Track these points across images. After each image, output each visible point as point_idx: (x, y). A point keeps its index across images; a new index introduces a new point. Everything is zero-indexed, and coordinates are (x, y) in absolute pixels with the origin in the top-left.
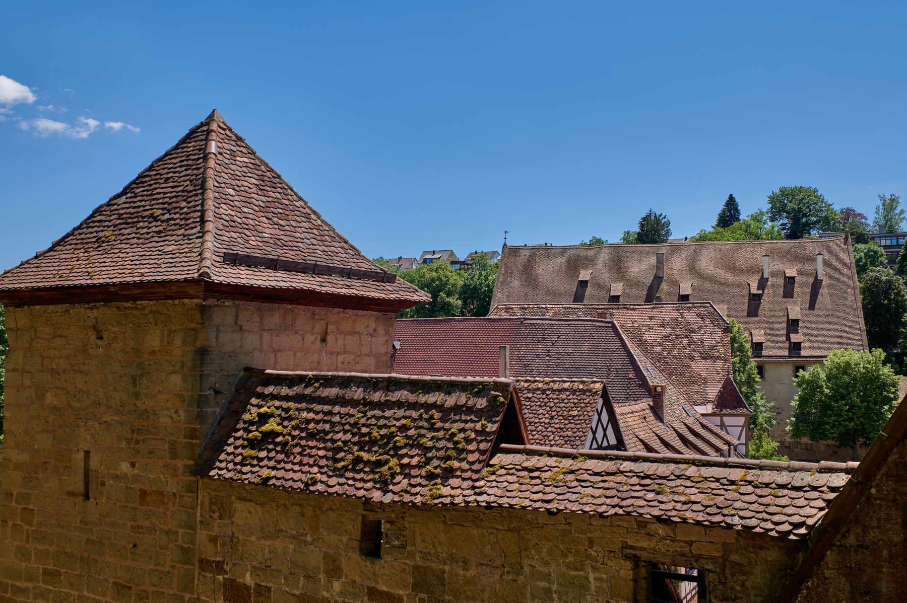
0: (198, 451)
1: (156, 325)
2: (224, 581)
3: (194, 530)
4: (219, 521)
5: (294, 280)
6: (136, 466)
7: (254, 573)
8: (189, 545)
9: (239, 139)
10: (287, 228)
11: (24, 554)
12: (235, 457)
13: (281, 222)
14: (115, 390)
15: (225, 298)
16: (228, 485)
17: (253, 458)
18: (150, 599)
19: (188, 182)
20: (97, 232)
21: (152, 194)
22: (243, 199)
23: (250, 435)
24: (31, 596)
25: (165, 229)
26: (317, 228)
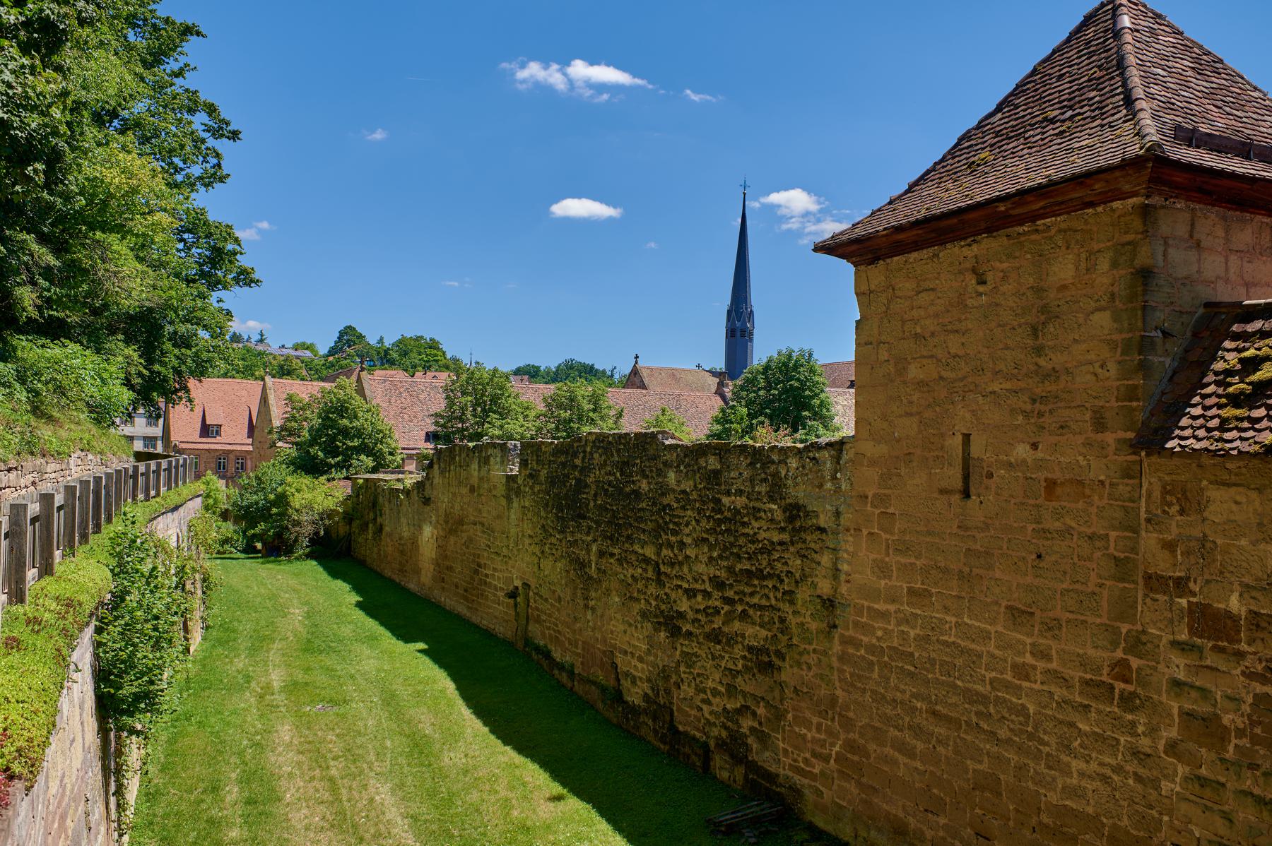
0: (1140, 417)
1: (1068, 248)
2: (1189, 607)
4: (1179, 518)
6: (1040, 447)
7: (1246, 595)
8: (1127, 554)
9: (1160, 16)
10: (1244, 120)
11: (882, 570)
12: (1207, 421)
14: (1007, 348)
15: (1176, 197)
16: (1194, 465)
17: (1242, 419)
18: (1064, 629)
19: (1095, 69)
20: (967, 159)
21: (1040, 98)
23: (1231, 389)
24: (893, 621)
25: (1069, 128)
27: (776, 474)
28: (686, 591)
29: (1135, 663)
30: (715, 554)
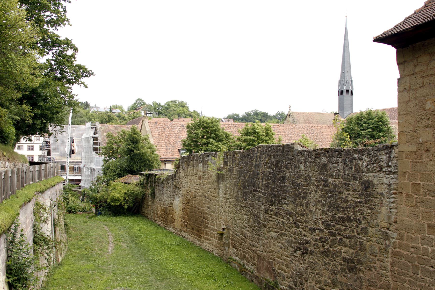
27: (357, 165)
28: (310, 229)
30: (325, 209)
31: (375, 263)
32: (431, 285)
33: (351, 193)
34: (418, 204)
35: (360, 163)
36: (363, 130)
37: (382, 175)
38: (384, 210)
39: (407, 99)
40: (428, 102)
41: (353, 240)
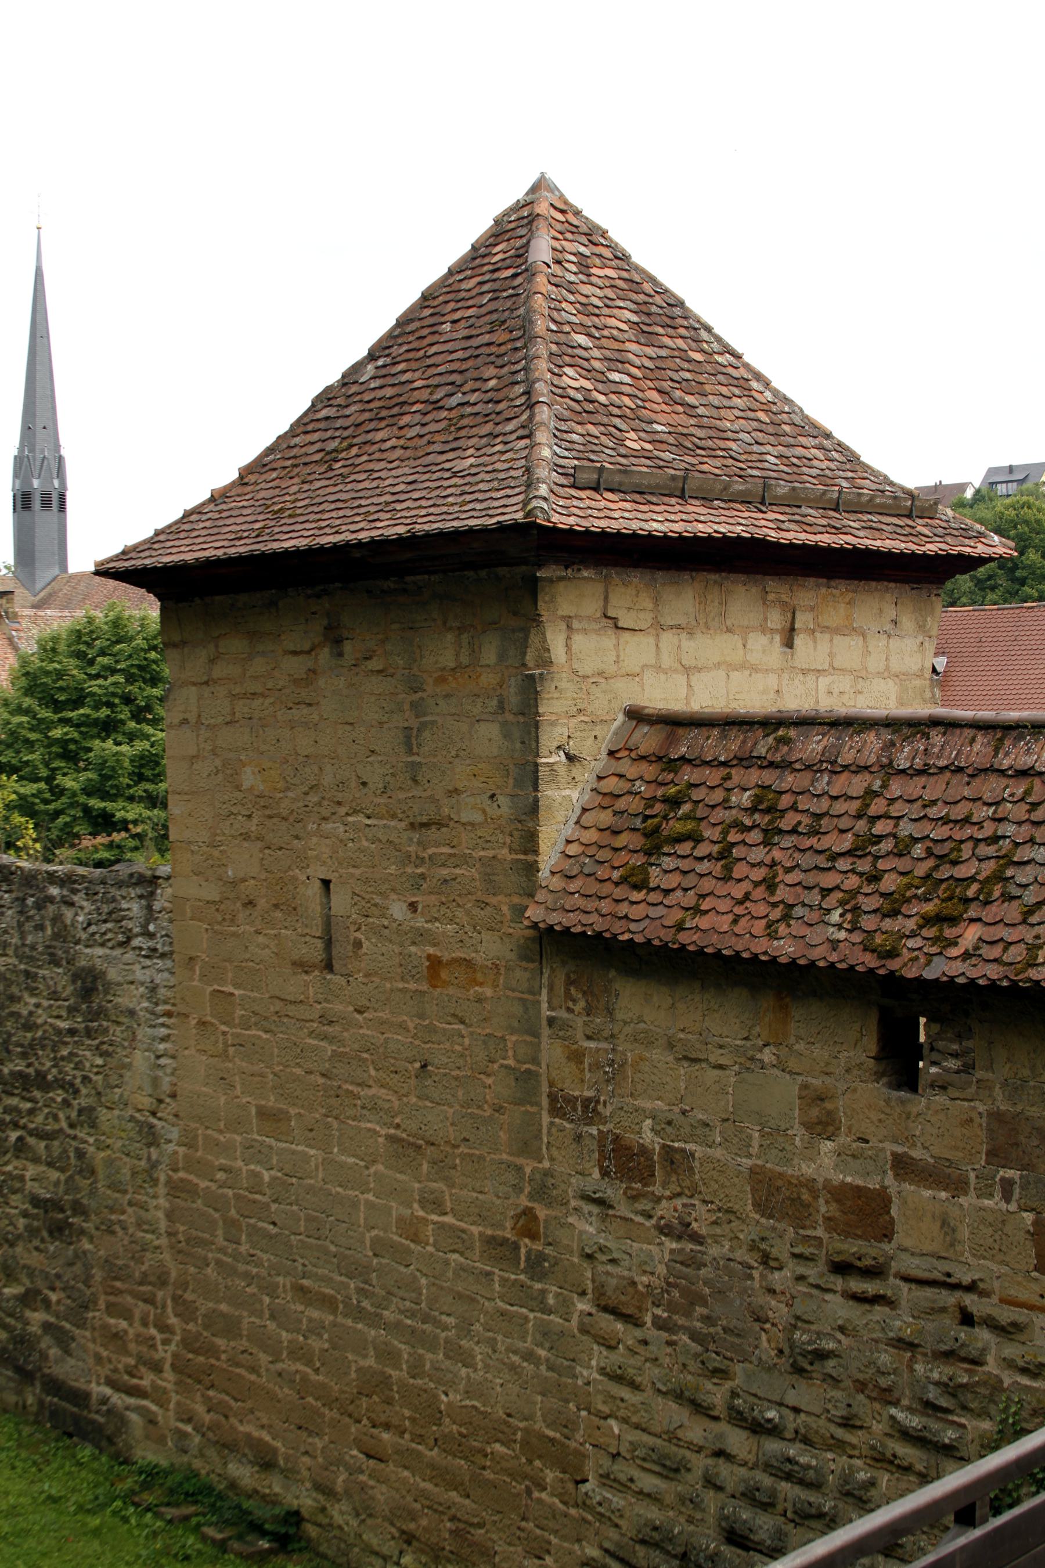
3: (536, 1035)
5: (723, 519)
10: (701, 411)
13: (690, 399)
22: (608, 353)
26: (765, 407)
29: (542, 1213)
31: (123, 1212)
32: (273, 1272)
33: (45, 1003)
34: (231, 1050)
35: (68, 914)
36: (98, 676)
37: (130, 956)
38: (140, 1059)
39: (192, 751)
40: (248, 770)
41: (56, 1143)
